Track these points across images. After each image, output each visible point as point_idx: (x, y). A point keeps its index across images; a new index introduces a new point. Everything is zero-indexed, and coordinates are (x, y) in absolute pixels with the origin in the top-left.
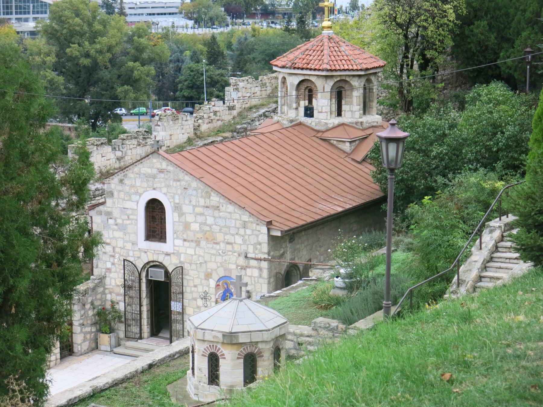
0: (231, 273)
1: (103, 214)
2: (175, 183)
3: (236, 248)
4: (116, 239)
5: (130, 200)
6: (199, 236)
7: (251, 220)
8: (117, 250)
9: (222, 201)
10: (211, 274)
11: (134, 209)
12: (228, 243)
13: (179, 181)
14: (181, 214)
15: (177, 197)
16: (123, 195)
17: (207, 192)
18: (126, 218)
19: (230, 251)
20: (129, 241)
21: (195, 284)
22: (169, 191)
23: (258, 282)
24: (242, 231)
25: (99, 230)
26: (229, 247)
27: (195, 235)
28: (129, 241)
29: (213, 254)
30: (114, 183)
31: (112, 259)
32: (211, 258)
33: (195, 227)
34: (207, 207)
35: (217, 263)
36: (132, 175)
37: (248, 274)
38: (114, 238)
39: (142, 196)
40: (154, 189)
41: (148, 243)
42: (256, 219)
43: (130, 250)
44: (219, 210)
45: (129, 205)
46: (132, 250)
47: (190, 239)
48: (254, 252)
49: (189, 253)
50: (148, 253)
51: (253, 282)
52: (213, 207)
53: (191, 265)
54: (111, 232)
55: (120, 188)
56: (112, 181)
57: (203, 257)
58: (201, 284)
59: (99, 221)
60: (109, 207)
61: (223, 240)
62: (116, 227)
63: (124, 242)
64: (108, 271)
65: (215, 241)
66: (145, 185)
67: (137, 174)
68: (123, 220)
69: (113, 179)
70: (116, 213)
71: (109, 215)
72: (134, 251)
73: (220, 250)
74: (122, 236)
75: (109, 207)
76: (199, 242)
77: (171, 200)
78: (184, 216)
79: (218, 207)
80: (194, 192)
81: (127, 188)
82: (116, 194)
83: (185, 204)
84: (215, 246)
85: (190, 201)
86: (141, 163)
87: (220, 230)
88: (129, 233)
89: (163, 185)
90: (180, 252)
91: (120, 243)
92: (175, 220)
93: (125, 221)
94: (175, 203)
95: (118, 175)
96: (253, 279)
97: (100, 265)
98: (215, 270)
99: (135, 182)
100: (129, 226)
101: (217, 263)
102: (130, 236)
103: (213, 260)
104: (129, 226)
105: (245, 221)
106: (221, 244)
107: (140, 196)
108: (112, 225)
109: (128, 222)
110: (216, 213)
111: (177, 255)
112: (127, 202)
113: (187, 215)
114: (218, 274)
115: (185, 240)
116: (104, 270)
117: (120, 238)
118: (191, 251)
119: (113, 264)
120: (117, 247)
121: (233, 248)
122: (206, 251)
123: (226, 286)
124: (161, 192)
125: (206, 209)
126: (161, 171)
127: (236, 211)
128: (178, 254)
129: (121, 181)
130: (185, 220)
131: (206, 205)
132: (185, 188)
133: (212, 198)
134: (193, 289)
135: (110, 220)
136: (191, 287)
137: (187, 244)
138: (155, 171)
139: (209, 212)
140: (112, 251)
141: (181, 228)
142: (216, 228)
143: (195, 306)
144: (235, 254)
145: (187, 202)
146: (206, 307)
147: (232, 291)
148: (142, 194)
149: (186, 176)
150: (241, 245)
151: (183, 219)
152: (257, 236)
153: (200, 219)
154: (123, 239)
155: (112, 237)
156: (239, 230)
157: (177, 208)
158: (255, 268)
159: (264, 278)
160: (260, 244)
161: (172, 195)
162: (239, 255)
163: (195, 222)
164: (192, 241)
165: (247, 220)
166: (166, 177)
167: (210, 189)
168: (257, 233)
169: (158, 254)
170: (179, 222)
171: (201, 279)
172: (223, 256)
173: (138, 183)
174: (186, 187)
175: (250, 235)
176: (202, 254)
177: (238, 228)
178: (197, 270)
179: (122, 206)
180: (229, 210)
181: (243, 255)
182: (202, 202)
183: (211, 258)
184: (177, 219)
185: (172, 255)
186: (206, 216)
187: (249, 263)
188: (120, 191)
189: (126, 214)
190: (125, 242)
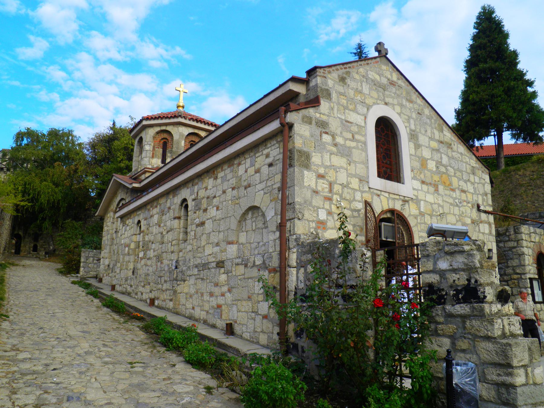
1: (314, 122)
2: (408, 104)
3: (470, 197)
4: (336, 169)
5: (355, 110)
6: (436, 178)
7: (477, 166)
8: (336, 188)
9: (453, 139)
11: (360, 126)
12: (463, 191)
13: (411, 101)
14: (418, 146)
15: (412, 121)
16: (345, 102)
17: (439, 125)
18: (350, 136)
19: (465, 201)
20: (355, 176)
22: (403, 112)
24: (472, 178)
25: (305, 149)
26: (464, 196)
27: (432, 177)
28: (355, 176)
29: (451, 204)
30: (330, 79)
31: (327, 206)
33: (432, 165)
34: (441, 142)
35: (455, 215)
36: (357, 77)
37: (481, 231)
38: (332, 166)
39: (372, 111)
40: (386, 104)
41: (383, 181)
43: (356, 190)
44: (452, 148)
45: (353, 117)
46: (360, 190)
47: (428, 180)
50: (381, 197)
52: (447, 143)
53: (431, 218)
54: (327, 156)
55: (341, 89)
56: (329, 76)
57: (442, 207)
59: (307, 134)
60: (324, 114)
61: (458, 186)
62: (334, 149)
63: (348, 176)
64: (322, 226)
66: (374, 94)
67: (363, 76)
68: (346, 139)
69: (329, 72)
70: (334, 125)
71: (323, 125)
72: (363, 192)
73: (456, 198)
74: (345, 166)
75: (324, 114)
76: (437, 185)
78: (420, 149)
80: (428, 121)
81: (351, 93)
82: (334, 95)
83: (421, 133)
85: (426, 131)
86: (368, 64)
87: (455, 173)
88: (355, 162)
89: (395, 102)
90: (419, 198)
91: (342, 178)
92: (411, 153)
93: (348, 142)
94: (411, 130)
95: (337, 70)
97: (307, 215)
99: (362, 86)
100: (354, 150)
101: (455, 215)
102: (356, 166)
103: (452, 212)
104: (354, 150)
105: (473, 167)
106: (457, 190)
107: (368, 109)
108: (328, 144)
109: (353, 144)
111: (416, 203)
112: (351, 113)
113: (423, 148)
116: (313, 225)
117: (341, 167)
118: (430, 198)
119: (330, 213)
120: (336, 183)
121: (467, 197)
122: (444, 199)
124: (394, 109)
125: (441, 144)
126: (392, 83)
127: (466, 153)
128: (417, 201)
129: (342, 80)
131: (442, 139)
132: (419, 113)
135: (325, 136)
137: (425, 187)
138: (384, 81)
139: (443, 149)
140: (327, 190)
141: (417, 165)
142: (451, 170)
145: (423, 131)
148: (372, 106)
150: (473, 194)
151: (419, 153)
152: (484, 185)
153: (437, 156)
154: (347, 170)
155: (328, 164)
157: (413, 136)
158: (486, 223)
159: (493, 236)
160: (486, 194)
162: (473, 207)
163: (432, 159)
164: (430, 184)
165: (474, 165)
166: (398, 92)
168: (483, 181)
169: (394, 199)
170: (415, 156)
172: (459, 207)
173: (366, 89)
174: (420, 112)
175: (478, 184)
176: (441, 202)
177: (469, 174)
179: (343, 118)
180: (460, 151)
182: (437, 135)
184: (413, 151)
185: (410, 202)
188: (341, 94)
189: (350, 131)
190: (350, 175)
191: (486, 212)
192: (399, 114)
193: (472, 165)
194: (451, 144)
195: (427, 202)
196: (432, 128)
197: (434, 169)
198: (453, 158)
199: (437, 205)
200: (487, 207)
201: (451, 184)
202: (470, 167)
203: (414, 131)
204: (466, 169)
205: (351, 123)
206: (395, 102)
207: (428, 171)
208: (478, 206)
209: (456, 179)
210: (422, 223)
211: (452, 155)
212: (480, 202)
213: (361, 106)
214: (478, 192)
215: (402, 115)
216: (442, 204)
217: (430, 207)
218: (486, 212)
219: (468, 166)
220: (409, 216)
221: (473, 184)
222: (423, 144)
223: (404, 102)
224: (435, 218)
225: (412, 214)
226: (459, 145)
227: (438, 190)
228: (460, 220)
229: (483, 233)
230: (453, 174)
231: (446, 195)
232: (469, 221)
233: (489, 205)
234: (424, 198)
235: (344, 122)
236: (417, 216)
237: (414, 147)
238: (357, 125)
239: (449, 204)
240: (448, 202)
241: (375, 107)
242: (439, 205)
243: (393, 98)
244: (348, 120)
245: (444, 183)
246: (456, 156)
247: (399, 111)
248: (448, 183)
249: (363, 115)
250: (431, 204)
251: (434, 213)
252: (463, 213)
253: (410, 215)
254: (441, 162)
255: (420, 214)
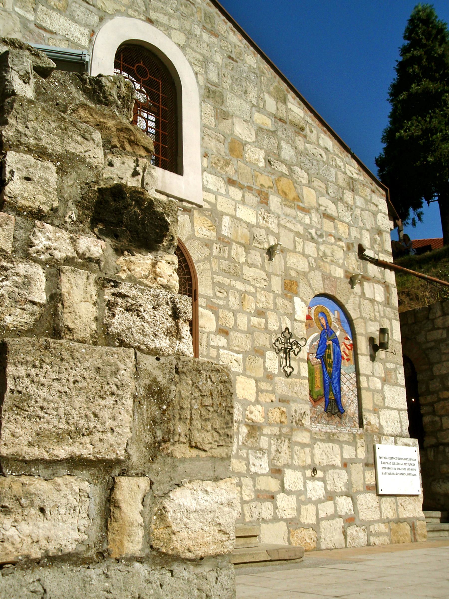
0: (336, 287)
2: (205, 36)
3: (343, 230)
7: (362, 178)
9: (310, 121)
10: (296, 283)
13: (214, 33)
17: (278, 90)
21: (260, 305)
22: (192, 45)
23: (385, 316)
24: (348, 196)
26: (328, 226)
29: (298, 234)
32: (295, 241)
34: (280, 120)
37: (367, 296)
40: (150, 21)
42: (369, 180)
44: (305, 136)
48: (372, 248)
49: (244, 218)
51: (377, 314)
52: (294, 124)
53: (247, 253)
57: (277, 236)
58: (275, 309)
61: (315, 205)
65: (301, 204)
73: (310, 226)
77: (197, 69)
78: (230, 121)
79: (302, 129)
84: (300, 214)
94: (207, 80)
96: (376, 307)
98: (305, 274)
103: (299, 248)
107: (101, 19)
110: (300, 142)
112: (54, 14)
114: (310, 286)
115: (231, 182)
121: (336, 228)
122: (282, 222)
123: (323, 321)
124: (169, 36)
125: (280, 123)
130: (232, 131)
131: (280, 115)
132: (230, 57)
133: (290, 105)
134: (255, 320)
136: (250, 314)
143: (260, 374)
144: (342, 244)
146: (288, 375)
147: (338, 333)
148: (112, 16)
149: (231, 34)
151: (224, 126)
152: (375, 215)
156: (343, 193)
158: (378, 282)
160: (380, 232)
161: (201, 58)
162: (349, 248)
165: (355, 176)
166: (183, 9)
167: (284, 86)
168: (374, 208)
171: (276, 296)
172: (317, 243)
174: (233, 56)
176: (273, 227)
177: (343, 189)
178: (263, 268)
179: (32, 18)
181: (356, 249)
183: (295, 241)
186: (279, 140)
187: (365, 269)
191: (377, 263)
192: (182, 48)
193: (349, 174)
194: (302, 129)
195: (240, 220)
196: (261, 91)
197: (262, 164)
198: (305, 153)
199: (263, 232)
200: (381, 255)
201: (299, 198)
202: (345, 177)
203: (216, 85)
204: (336, 178)
205: (51, 32)
206: (175, 23)
207: (246, 163)
208: (361, 249)
209: (313, 192)
210: (224, 258)
211: (306, 149)
212: (366, 243)
213: (82, 9)
214: (361, 225)
215: (188, 50)
216: (276, 230)
217: (246, 231)
218: (377, 263)
219: (341, 176)
220: (188, 239)
221: (349, 208)
222: (237, 113)
223: (197, 30)
224: (258, 254)
225: (198, 236)
226: (322, 135)
227: (267, 204)
228: (318, 268)
229: (372, 301)
230: (305, 181)
231: (286, 215)
232: (339, 273)
233: (386, 252)
234: (231, 212)
235: (32, 26)
236: (212, 242)
237: (213, 113)
238: (68, 40)
239: (292, 235)
240: (290, 230)
241: (118, 19)
242: (268, 231)
243: (171, 16)
244: (44, 25)
245: (285, 194)
246: (315, 151)
247: (182, 42)
248: (292, 195)
249: (86, 26)
250: (249, 225)
251: (255, 244)
252: (325, 255)
253: (192, 237)
254: (279, 155)
255: (219, 239)
